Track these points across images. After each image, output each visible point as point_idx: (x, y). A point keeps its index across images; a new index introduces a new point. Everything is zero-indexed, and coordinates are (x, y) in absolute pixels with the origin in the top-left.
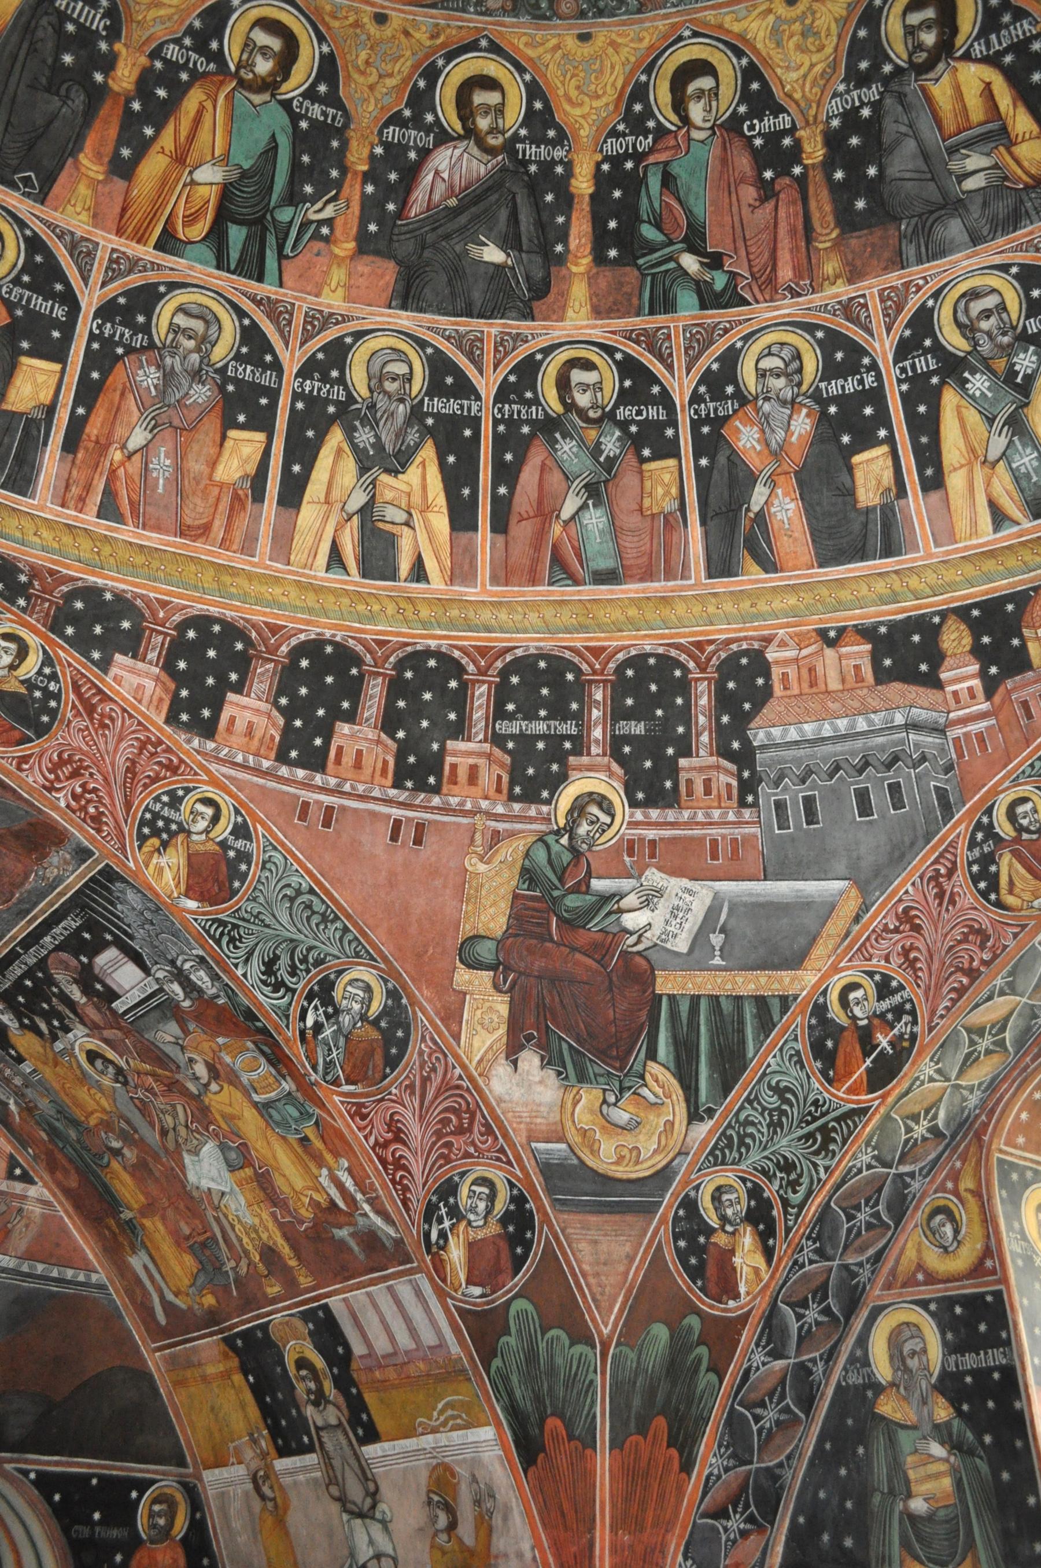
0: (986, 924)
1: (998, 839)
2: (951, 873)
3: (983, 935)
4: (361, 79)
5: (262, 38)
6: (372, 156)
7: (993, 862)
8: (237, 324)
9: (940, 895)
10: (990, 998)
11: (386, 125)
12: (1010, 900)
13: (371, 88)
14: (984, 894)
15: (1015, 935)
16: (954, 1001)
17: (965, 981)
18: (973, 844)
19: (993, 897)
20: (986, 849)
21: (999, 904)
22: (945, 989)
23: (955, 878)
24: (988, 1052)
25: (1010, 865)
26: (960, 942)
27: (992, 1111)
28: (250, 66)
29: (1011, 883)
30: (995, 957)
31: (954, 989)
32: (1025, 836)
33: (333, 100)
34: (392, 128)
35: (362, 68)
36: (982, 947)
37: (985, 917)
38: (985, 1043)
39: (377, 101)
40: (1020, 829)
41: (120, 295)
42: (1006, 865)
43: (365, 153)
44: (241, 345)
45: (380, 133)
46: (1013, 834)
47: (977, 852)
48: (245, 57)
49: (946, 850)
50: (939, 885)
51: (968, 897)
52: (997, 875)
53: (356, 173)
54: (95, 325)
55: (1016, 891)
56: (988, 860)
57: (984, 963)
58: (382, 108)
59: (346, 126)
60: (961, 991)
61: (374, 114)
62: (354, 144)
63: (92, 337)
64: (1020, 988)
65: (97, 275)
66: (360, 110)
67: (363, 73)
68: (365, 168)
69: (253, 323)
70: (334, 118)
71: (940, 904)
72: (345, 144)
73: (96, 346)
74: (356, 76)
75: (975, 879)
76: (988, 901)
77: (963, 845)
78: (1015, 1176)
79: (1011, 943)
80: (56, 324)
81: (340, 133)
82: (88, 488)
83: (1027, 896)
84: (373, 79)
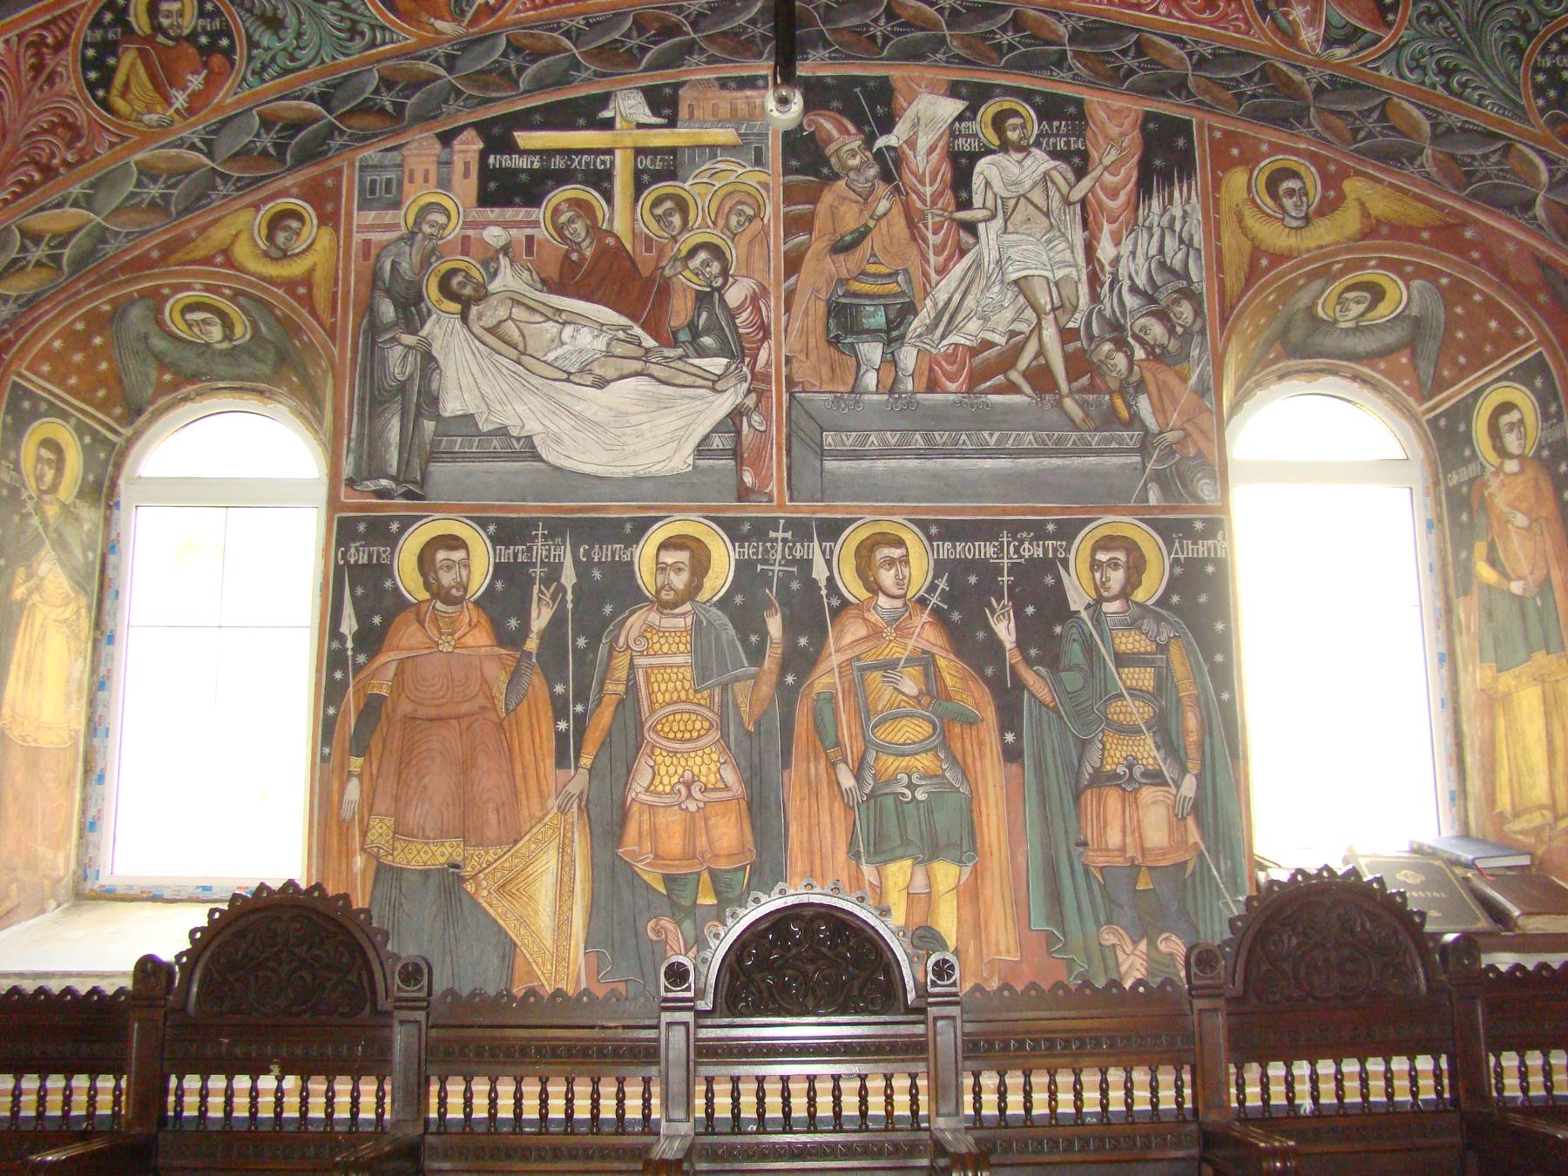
0: (82, 120)
1: (128, 30)
2: (59, 46)
3: (75, 132)
7: (114, 53)
9: (37, 69)
10: (59, 205)
12: (119, 104)
14: (92, 86)
15: (112, 145)
16: (16, 196)
17: (37, 176)
18: (97, 23)
19: (101, 93)
20: (111, 36)
21: (105, 104)
22: (11, 179)
23: (62, 54)
24: (39, 264)
25: (133, 65)
26: (45, 131)
27: (24, 330)
29: (127, 85)
30: (81, 161)
31: (20, 182)
32: (160, 38)
36: (69, 146)
37: (84, 112)
38: (37, 253)
40: (157, 28)
42: (127, 63)
46: (148, 30)
47: (99, 35)
49: (61, 17)
50: (39, 55)
51: (70, 80)
52: (114, 70)
55: (130, 96)
56: (109, 48)
57: (65, 163)
60: (28, 187)
64: (97, 204)
71: (35, 79)
75: (87, 65)
76: (94, 97)
77: (84, 19)
78: (26, 405)
79: (104, 152)
83: (139, 107)
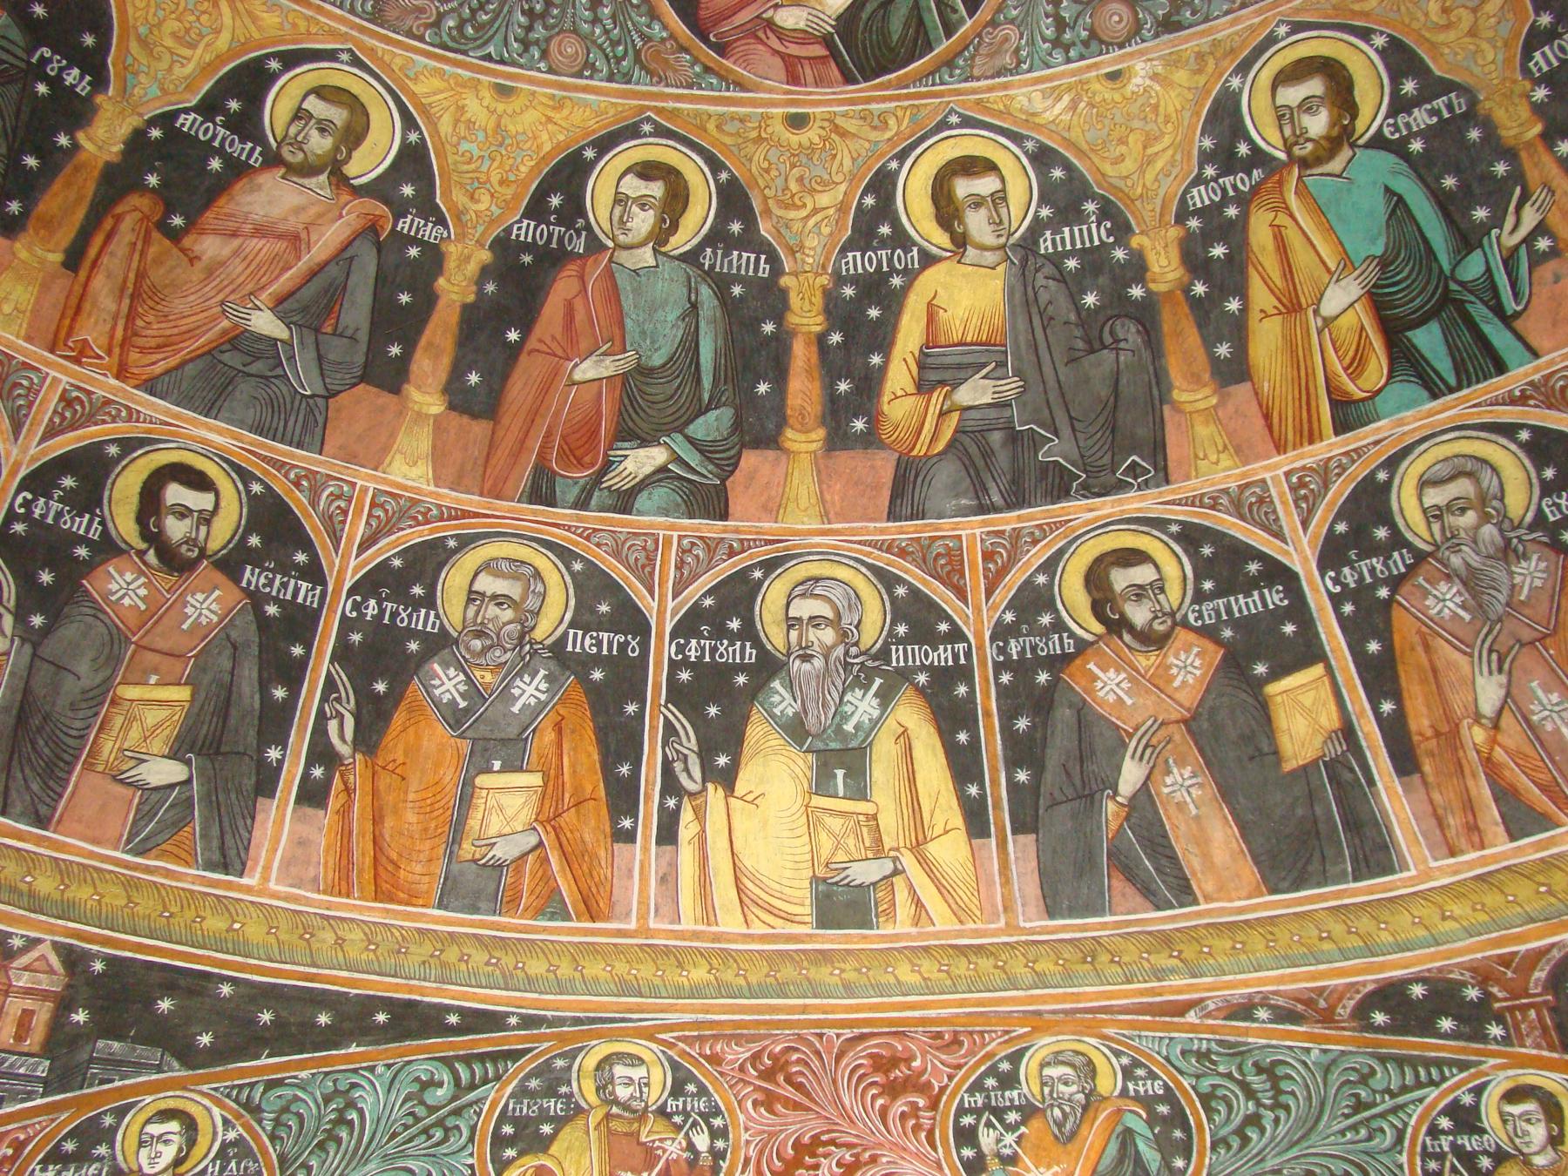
4: (1451, 35)
5: (1291, 95)
6: (1538, 109)
8: (1513, 447)
11: (1527, 54)
13: (1473, 33)
28: (1301, 136)
33: (1433, 87)
34: (1537, 55)
35: (1443, 22)
39: (1491, 41)
41: (1334, 522)
43: (1524, 112)
44: (1539, 470)
45: (1526, 71)
48: (1287, 132)
53: (1529, 145)
54: (1329, 583)
58: (1506, 45)
59: (1473, 102)
61: (1500, 57)
62: (1500, 115)
63: (1336, 601)
65: (1289, 518)
66: (1477, 70)
67: (1448, 27)
68: (1538, 128)
69: (1534, 429)
70: (1450, 107)
72: (1488, 126)
73: (1348, 608)
74: (1441, 38)
80: (1280, 616)
81: (1470, 116)
82: (1469, 806)
84: (1466, 19)
